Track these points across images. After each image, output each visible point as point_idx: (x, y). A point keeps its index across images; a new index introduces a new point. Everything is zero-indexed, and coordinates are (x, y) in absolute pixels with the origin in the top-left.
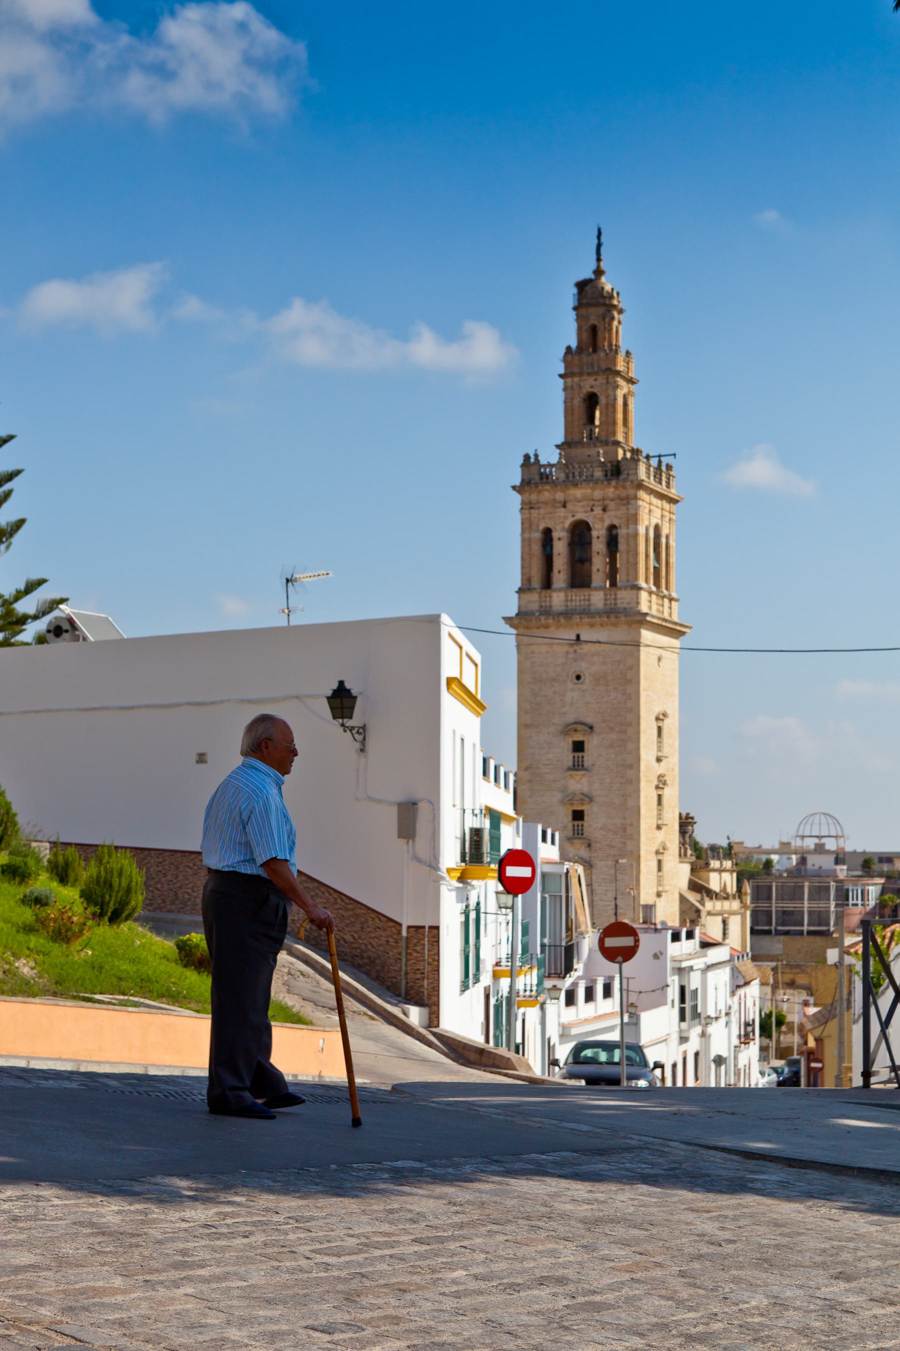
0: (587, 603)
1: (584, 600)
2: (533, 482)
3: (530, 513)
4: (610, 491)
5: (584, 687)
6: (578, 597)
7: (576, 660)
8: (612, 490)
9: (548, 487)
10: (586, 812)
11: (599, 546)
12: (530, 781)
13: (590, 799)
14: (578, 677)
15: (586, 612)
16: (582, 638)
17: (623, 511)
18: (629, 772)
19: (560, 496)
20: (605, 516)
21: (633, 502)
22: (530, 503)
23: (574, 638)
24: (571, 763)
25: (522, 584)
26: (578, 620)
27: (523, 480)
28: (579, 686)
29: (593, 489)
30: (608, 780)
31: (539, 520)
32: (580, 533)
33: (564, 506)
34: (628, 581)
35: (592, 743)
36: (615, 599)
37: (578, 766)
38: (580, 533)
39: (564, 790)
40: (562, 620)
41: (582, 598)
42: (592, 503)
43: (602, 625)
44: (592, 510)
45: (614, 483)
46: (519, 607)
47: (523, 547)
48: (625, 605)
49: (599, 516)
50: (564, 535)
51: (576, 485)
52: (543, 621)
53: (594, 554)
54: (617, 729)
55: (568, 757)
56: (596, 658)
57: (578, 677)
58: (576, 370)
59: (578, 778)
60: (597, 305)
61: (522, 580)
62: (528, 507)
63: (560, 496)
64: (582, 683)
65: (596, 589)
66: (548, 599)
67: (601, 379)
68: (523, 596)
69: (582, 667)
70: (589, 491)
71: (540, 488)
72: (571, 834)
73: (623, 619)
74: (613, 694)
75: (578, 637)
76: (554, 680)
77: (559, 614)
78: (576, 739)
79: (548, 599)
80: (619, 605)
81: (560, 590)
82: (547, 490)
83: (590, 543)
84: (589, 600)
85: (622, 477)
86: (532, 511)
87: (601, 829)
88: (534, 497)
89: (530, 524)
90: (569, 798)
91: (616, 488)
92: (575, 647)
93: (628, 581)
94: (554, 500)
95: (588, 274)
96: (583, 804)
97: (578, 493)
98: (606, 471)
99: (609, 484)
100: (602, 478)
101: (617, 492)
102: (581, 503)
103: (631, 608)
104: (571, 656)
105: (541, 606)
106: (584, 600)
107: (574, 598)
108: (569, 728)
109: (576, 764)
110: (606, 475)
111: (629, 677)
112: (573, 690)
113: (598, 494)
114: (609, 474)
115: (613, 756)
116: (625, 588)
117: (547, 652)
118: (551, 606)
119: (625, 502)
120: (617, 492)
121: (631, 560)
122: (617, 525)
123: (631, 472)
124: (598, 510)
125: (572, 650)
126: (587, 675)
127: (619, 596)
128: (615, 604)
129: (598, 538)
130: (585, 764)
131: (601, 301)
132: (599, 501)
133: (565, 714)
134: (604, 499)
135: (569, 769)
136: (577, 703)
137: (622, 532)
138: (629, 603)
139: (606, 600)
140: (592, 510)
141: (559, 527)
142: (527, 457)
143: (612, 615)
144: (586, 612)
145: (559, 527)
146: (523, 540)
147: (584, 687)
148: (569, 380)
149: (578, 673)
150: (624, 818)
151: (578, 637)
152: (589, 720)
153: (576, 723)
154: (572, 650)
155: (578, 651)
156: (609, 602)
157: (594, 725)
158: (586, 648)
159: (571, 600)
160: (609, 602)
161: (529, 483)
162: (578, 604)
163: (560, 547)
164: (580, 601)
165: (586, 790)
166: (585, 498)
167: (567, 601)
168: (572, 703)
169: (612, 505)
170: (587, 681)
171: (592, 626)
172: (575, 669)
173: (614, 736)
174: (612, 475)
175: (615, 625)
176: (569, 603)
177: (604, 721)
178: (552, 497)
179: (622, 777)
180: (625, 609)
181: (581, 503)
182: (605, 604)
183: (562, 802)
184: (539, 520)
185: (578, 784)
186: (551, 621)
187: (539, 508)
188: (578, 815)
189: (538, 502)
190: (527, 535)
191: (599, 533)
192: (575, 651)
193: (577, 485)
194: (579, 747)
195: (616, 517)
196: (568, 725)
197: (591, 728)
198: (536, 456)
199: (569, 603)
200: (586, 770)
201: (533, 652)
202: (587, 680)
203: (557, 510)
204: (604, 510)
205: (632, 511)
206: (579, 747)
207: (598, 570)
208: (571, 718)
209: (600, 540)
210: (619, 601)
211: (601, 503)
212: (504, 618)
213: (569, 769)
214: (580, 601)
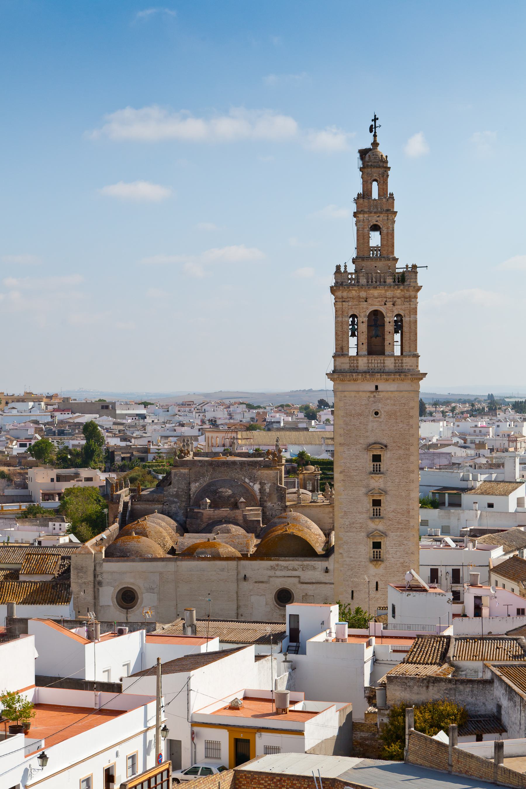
0: (382, 365)
1: (381, 363)
2: (344, 284)
3: (343, 305)
4: (398, 293)
5: (381, 420)
6: (376, 361)
7: (375, 402)
8: (399, 291)
9: (356, 288)
10: (382, 501)
11: (389, 327)
12: (343, 480)
13: (386, 492)
14: (376, 413)
15: (382, 372)
16: (380, 389)
17: (407, 305)
18: (411, 475)
19: (363, 294)
20: (394, 308)
21: (413, 300)
22: (342, 298)
23: (373, 389)
24: (372, 469)
25: (336, 351)
26: (379, 377)
27: (336, 283)
28: (377, 419)
29: (386, 291)
30: (397, 480)
31: (348, 309)
32: (376, 319)
33: (366, 301)
34: (410, 351)
35: (386, 456)
36: (402, 363)
37: (377, 471)
38: (376, 319)
39: (368, 486)
40: (368, 376)
41: (379, 361)
42: (385, 299)
43: (394, 380)
44: (385, 304)
45: (402, 287)
46: (335, 366)
47: (336, 327)
48: (408, 367)
49: (390, 308)
50: (366, 319)
51: (375, 288)
52: (354, 377)
53: (386, 333)
54: (403, 447)
55: (370, 465)
56: (389, 401)
57: (376, 413)
58: (366, 210)
59: (377, 479)
60: (379, 167)
61: (336, 349)
62: (341, 300)
63: (363, 294)
64: (379, 417)
65: (389, 356)
66: (355, 362)
67: (383, 217)
68: (337, 359)
69: (379, 407)
70: (383, 291)
71: (351, 288)
72: (372, 516)
73: (410, 377)
74: (401, 425)
75: (377, 387)
76: (361, 415)
77: (365, 372)
78: (375, 453)
79: (355, 362)
80: (404, 367)
81: (364, 356)
82: (355, 290)
83: (383, 325)
84: (384, 363)
85: (405, 284)
86: (344, 303)
87: (393, 511)
88: (345, 294)
89: (342, 312)
90: (370, 492)
91: (401, 290)
92: (375, 394)
93: (410, 351)
94: (359, 297)
95: (368, 145)
96: (380, 496)
97: (376, 293)
98: (394, 279)
99: (398, 288)
100: (392, 284)
101: (403, 293)
102: (377, 299)
103: (413, 369)
104: (372, 399)
105: (350, 366)
106: (381, 363)
107: (373, 361)
108: (369, 447)
109: (375, 469)
110: (394, 282)
111: (411, 414)
112: (373, 421)
113: (389, 294)
114: (397, 281)
115: (400, 465)
116: (409, 356)
117: (355, 397)
118: (357, 366)
119: (408, 300)
120: (403, 293)
121: (412, 338)
122: (403, 315)
123: (412, 280)
124: (389, 304)
125: (372, 395)
126: (383, 412)
127: (404, 361)
128: (402, 366)
129: (390, 322)
130: (382, 470)
131: (381, 164)
132: (390, 298)
133: (367, 437)
134: (393, 298)
135: (371, 473)
136: (376, 430)
137: (406, 319)
138: (411, 366)
139: (395, 363)
140: (385, 304)
141: (362, 314)
142: (338, 267)
143: (402, 374)
144: (382, 372)
145: (362, 314)
146: (336, 323)
147: (381, 420)
148: (361, 216)
149: (377, 411)
150: (408, 505)
151: (377, 387)
152: (384, 442)
153: (375, 443)
154: (372, 395)
155: (377, 396)
156: (397, 365)
157: (388, 445)
158: (382, 395)
159: (371, 363)
160: (397, 365)
161: (342, 284)
162: (376, 365)
163: (363, 328)
164: (378, 363)
165: (382, 486)
166: (380, 296)
167: (368, 363)
168: (373, 430)
169: (399, 301)
170: (383, 416)
171: (387, 380)
172: (375, 408)
173: (401, 452)
174: (399, 282)
175: (402, 380)
176: (370, 365)
177: (394, 442)
178: (357, 295)
179: (407, 479)
180: (408, 369)
181: (377, 299)
182: (395, 366)
183: (366, 494)
184: (348, 309)
185: (377, 482)
186: (360, 377)
187: (348, 301)
188: (377, 503)
189: (348, 298)
190: (340, 319)
191: (390, 319)
192: (374, 396)
193: (376, 287)
194: (377, 458)
195: (401, 309)
196: (370, 445)
197: (386, 446)
198: (346, 266)
199: (370, 365)
200: (382, 473)
201: (345, 396)
202: (382, 414)
203: (361, 303)
204: (394, 305)
205: (413, 306)
206: (377, 458)
207: (390, 344)
208: (372, 440)
209: (391, 324)
210: (404, 365)
211: (391, 300)
212: (327, 374)
213: (371, 473)
214: (378, 363)
